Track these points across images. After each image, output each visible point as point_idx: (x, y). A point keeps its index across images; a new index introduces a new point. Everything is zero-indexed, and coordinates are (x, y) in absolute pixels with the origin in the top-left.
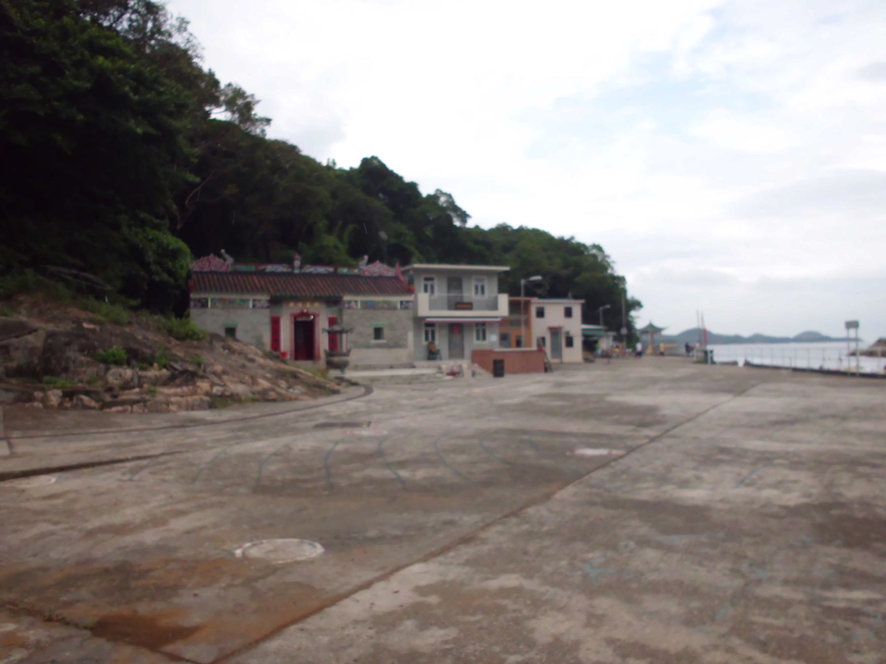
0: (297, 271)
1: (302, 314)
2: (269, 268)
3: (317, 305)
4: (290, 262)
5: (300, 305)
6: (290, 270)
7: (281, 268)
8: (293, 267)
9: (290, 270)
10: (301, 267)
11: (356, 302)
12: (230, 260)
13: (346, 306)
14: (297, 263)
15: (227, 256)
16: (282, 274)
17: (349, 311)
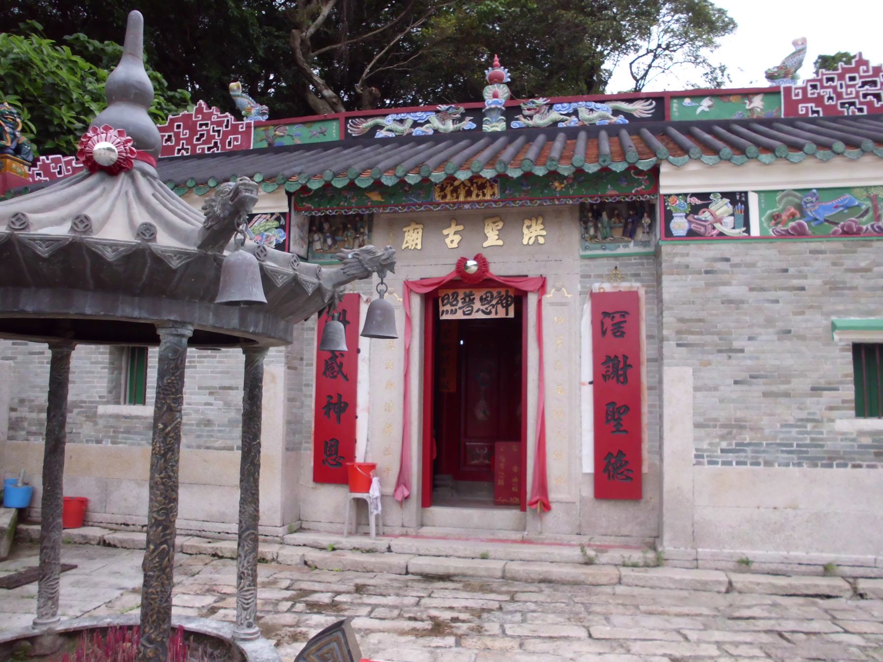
0: (495, 125)
1: (463, 282)
2: (390, 124)
3: (533, 233)
4: (470, 95)
5: (452, 237)
6: (468, 124)
7: (437, 121)
8: (478, 115)
9: (468, 124)
10: (511, 112)
11: (738, 199)
12: (254, 111)
13: (680, 225)
14: (496, 95)
15: (244, 101)
16: (438, 137)
17: (698, 254)
